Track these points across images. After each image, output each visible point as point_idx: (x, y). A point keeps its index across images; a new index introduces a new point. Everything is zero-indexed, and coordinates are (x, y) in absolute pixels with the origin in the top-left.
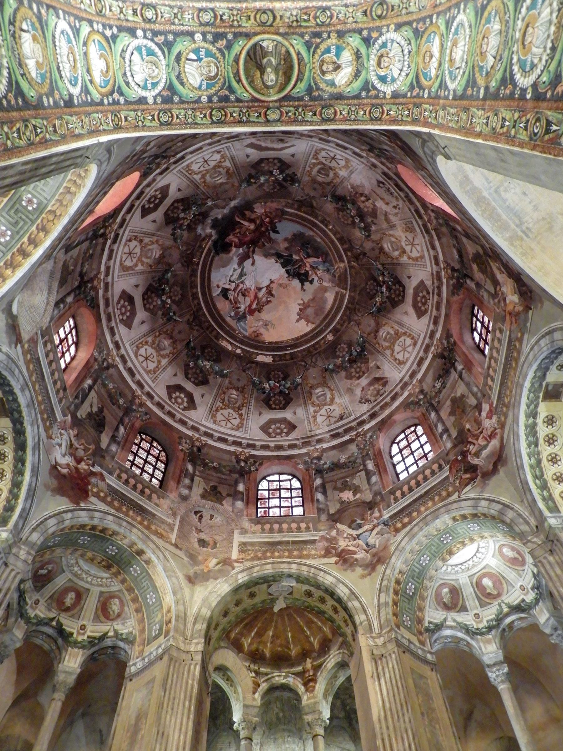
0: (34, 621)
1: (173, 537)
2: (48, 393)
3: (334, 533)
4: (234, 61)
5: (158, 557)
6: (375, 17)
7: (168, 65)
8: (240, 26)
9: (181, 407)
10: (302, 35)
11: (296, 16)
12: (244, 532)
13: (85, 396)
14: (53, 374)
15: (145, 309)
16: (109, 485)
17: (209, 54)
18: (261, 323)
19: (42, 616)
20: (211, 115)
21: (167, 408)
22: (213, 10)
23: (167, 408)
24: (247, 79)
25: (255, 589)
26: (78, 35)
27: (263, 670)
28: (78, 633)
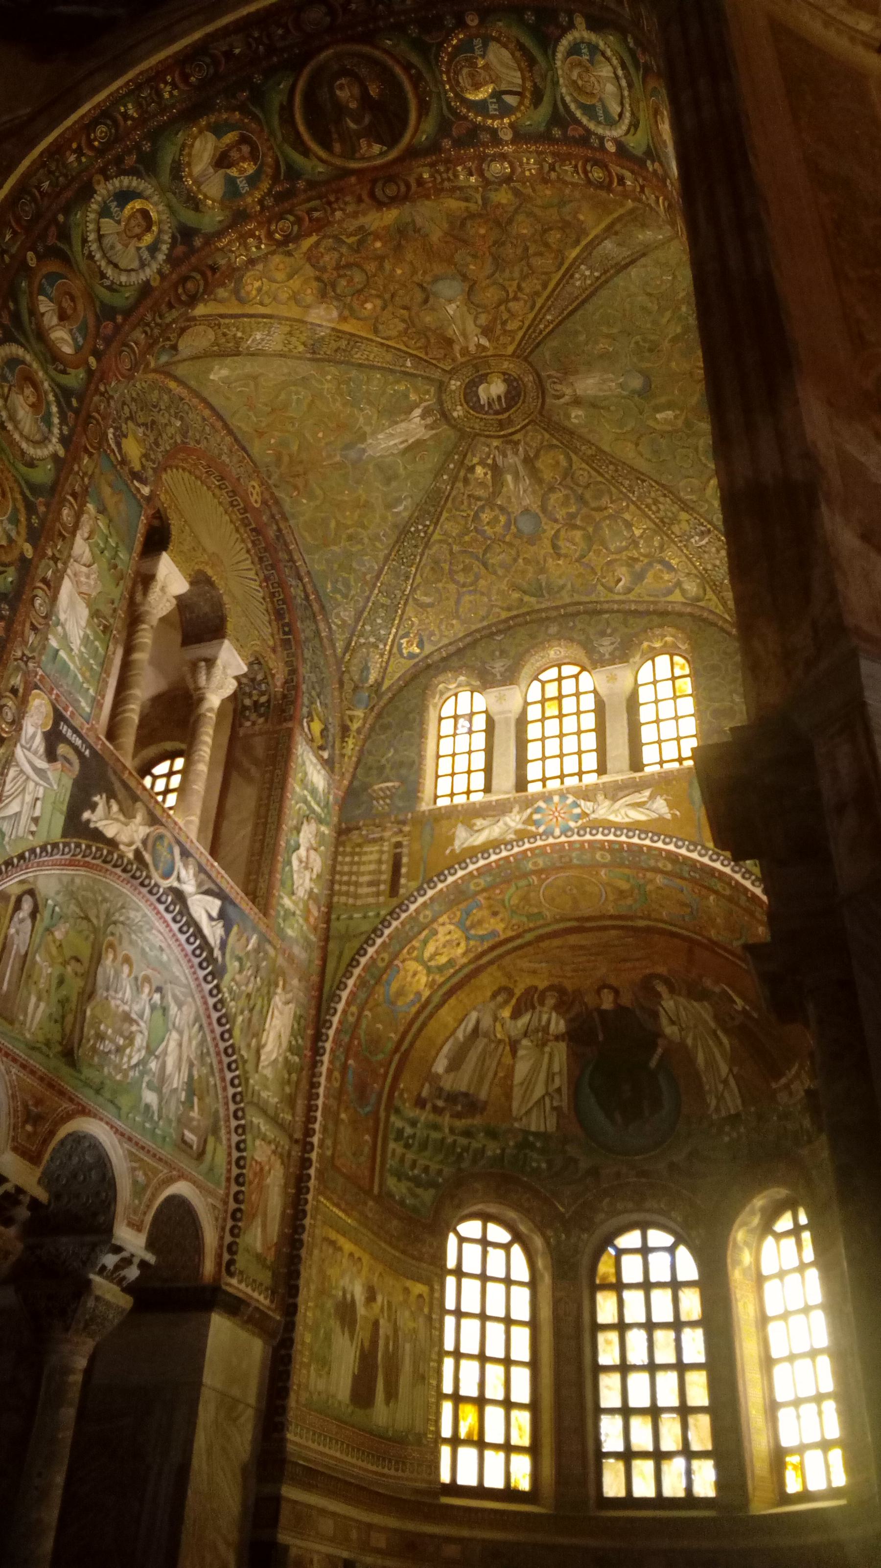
4: (428, 104)
6: (194, 274)
7: (555, 84)
8: (432, 165)
10: (312, 184)
11: (333, 211)
17: (481, 107)
24: (393, 75)
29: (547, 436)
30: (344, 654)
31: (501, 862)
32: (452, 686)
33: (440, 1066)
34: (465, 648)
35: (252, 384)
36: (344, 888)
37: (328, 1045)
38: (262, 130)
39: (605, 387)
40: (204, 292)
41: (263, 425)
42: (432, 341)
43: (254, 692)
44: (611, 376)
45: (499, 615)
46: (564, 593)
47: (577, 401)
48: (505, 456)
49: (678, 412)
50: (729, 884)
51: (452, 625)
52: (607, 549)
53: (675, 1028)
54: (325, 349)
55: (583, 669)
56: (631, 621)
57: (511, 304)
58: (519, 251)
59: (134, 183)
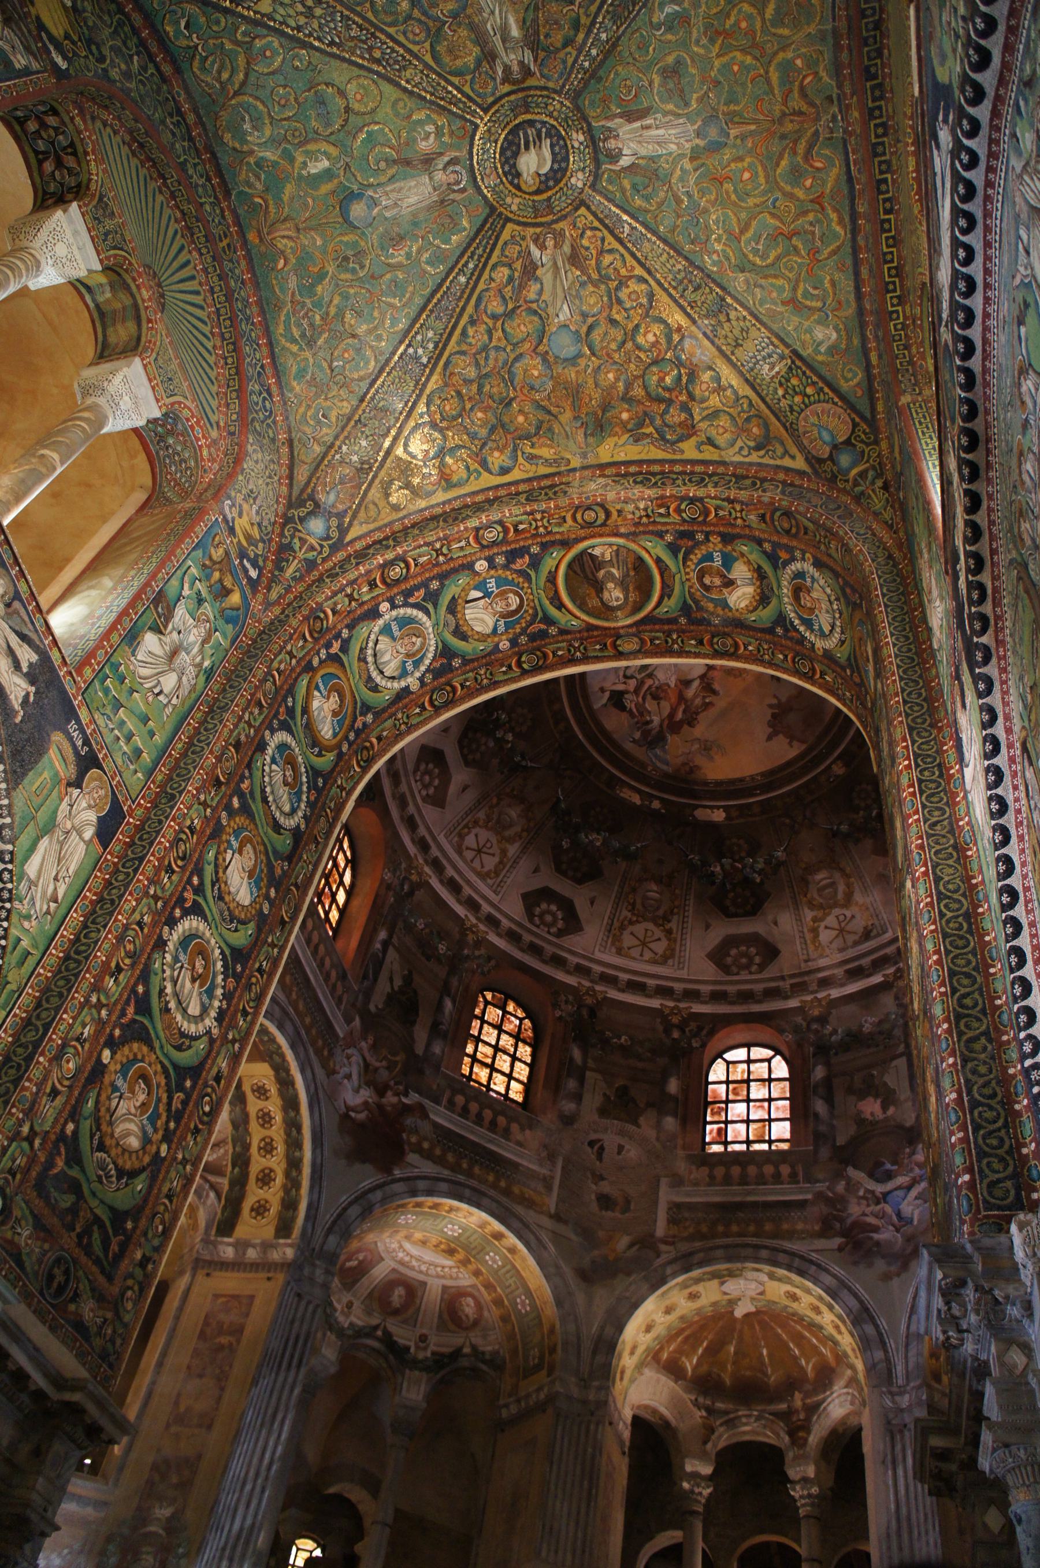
0: (350, 1332)
1: (551, 1203)
2: (319, 1002)
3: (841, 1187)
4: (548, 581)
5: (527, 1245)
7: (436, 625)
8: (549, 533)
9: (553, 930)
10: (660, 535)
11: (645, 509)
12: (677, 1181)
13: (379, 964)
14: (321, 965)
15: (467, 764)
16: (436, 1125)
18: (696, 746)
19: (360, 1323)
20: (519, 664)
21: (527, 938)
22: (500, 522)
23: (527, 938)
24: (573, 600)
25: (699, 1288)
26: (293, 718)
27: (719, 1405)
28: (417, 1347)
29: (467, 89)
35: (800, 292)
38: (691, 587)
39: (393, 196)
40: (776, 510)
41: (811, 217)
42: (593, 262)
44: (388, 214)
47: (428, 161)
48: (521, 63)
49: (304, 172)
54: (710, 297)
57: (500, 310)
58: (487, 388)
59: (797, 622)
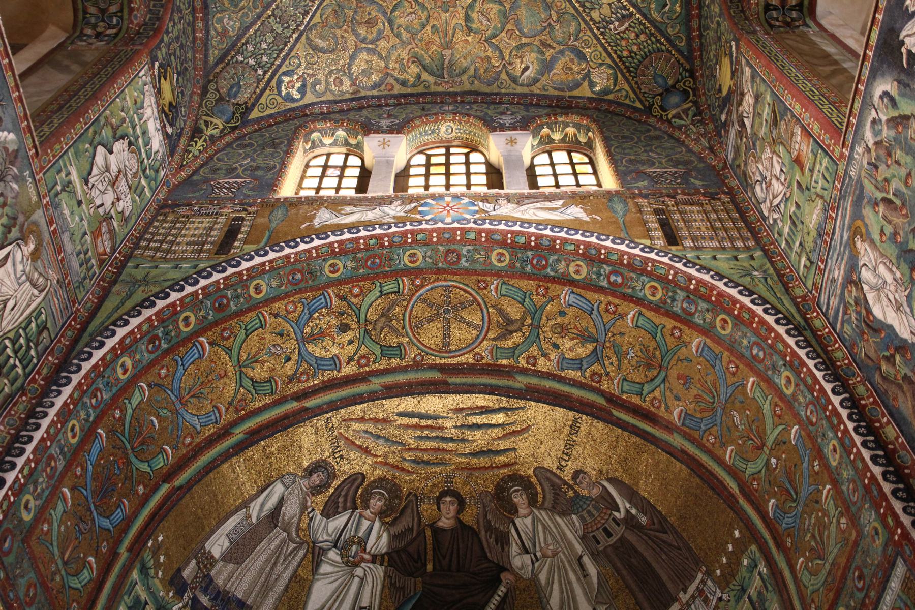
30: (216, 64)
31: (372, 242)
32: (328, 141)
33: (217, 545)
34: (349, 110)
36: (152, 245)
37: (76, 378)
43: (101, 24)
45: (392, 89)
46: (465, 77)
50: (663, 279)
51: (341, 82)
52: (519, 30)
53: (527, 558)
55: (474, 149)
56: (532, 109)
